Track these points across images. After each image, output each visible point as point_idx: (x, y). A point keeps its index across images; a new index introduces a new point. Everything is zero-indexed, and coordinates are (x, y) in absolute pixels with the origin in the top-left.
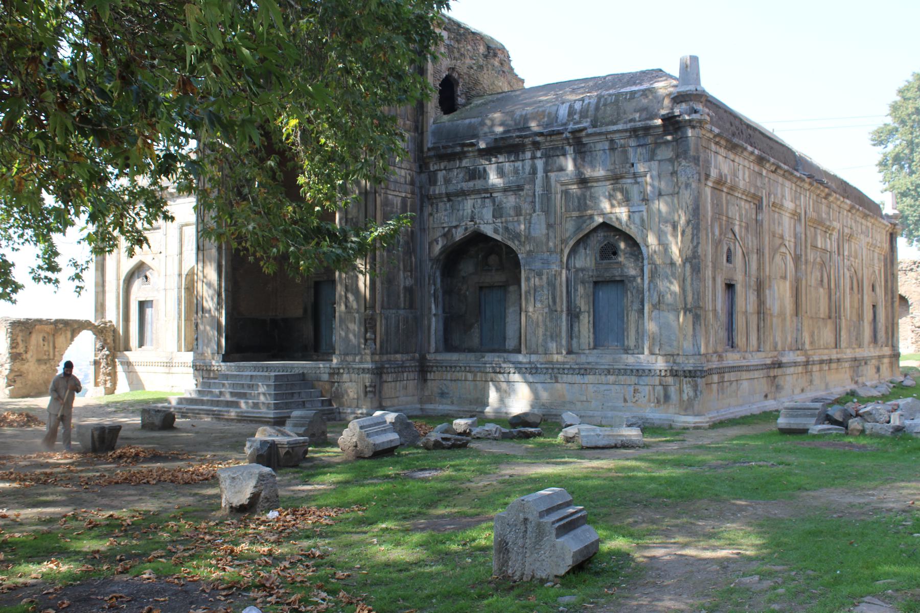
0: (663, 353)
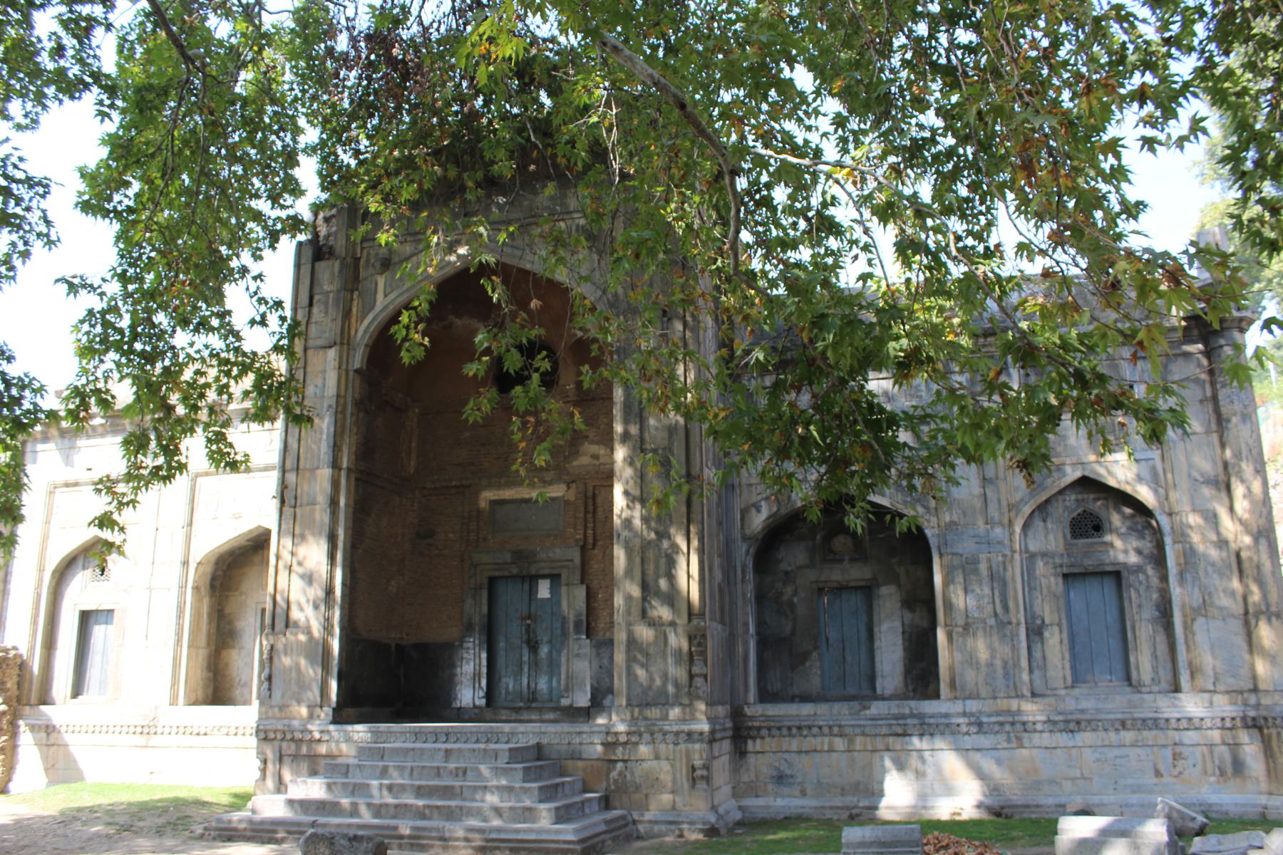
0: (1220, 688)
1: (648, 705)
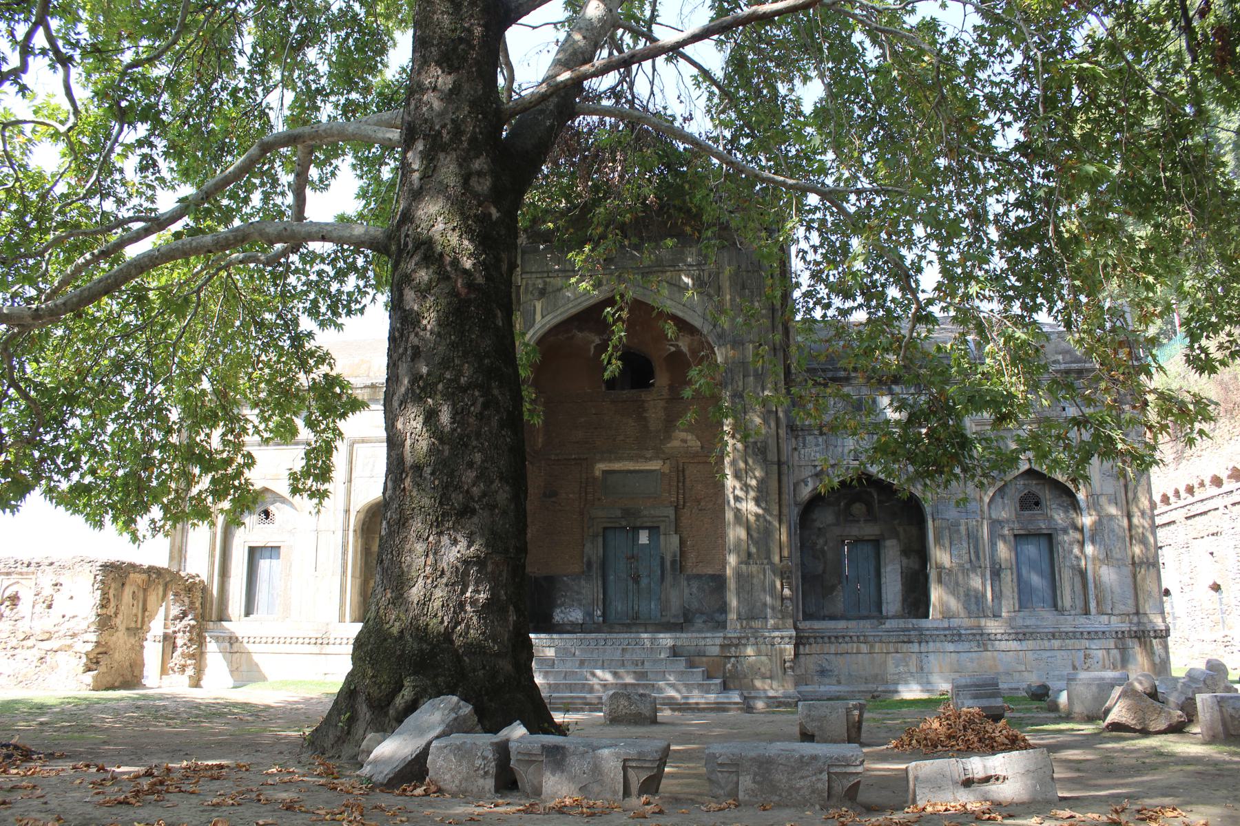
1: (753, 618)
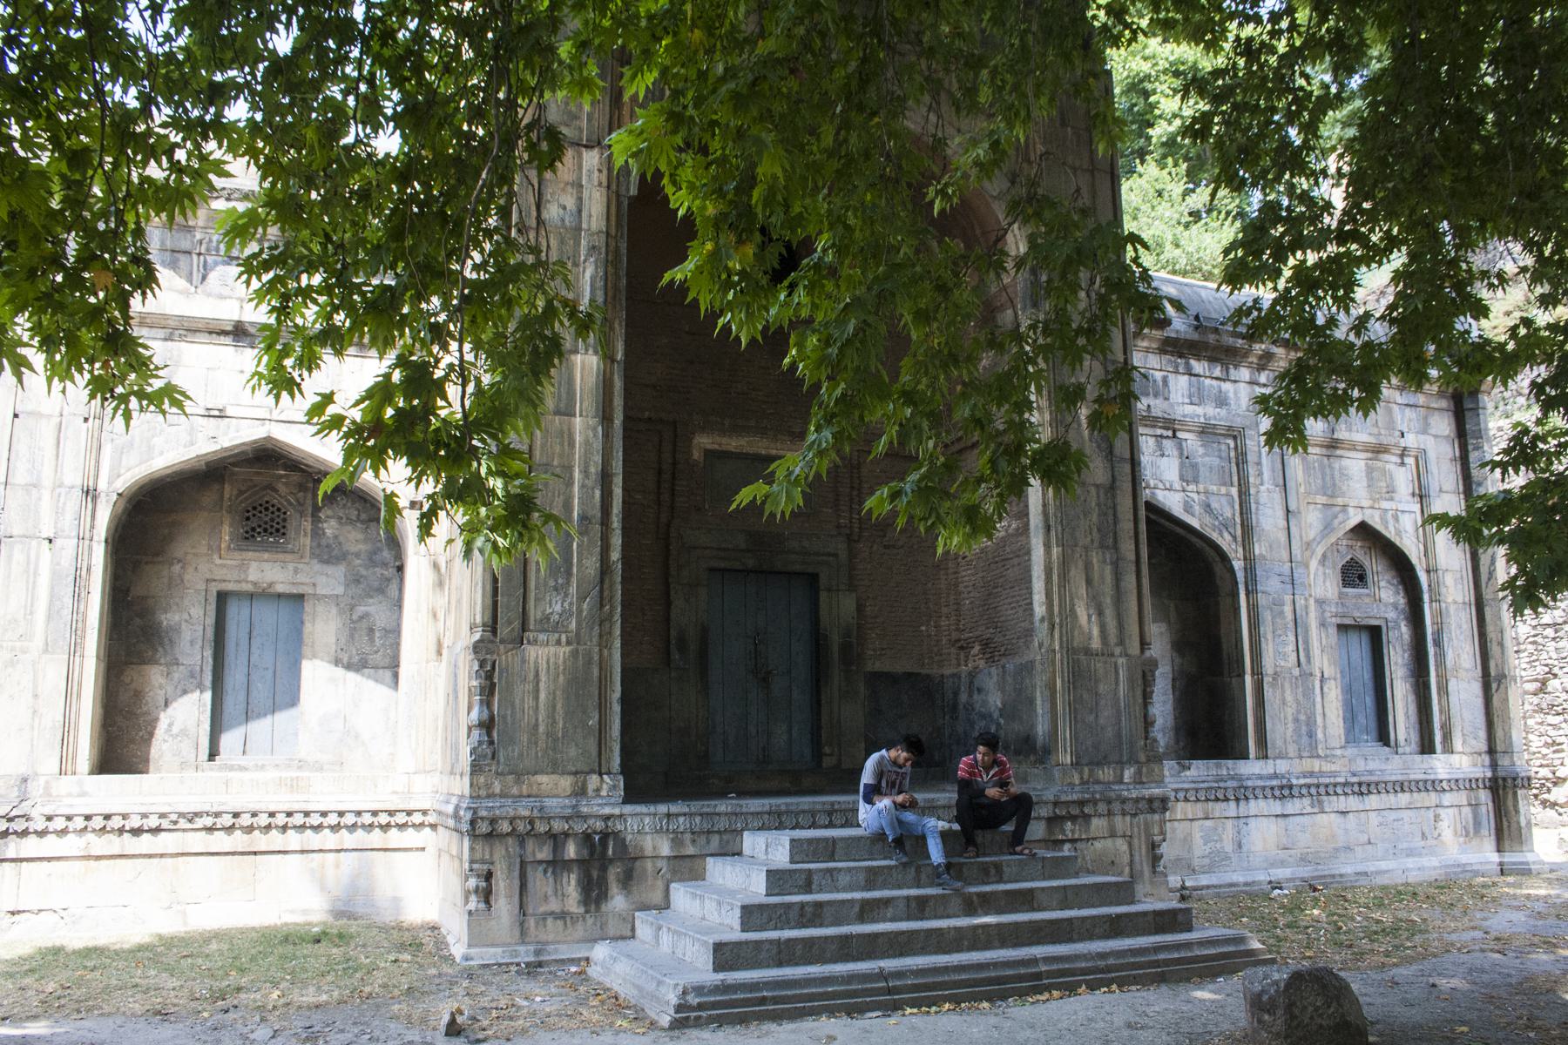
0: (1468, 750)
1: (1099, 764)
